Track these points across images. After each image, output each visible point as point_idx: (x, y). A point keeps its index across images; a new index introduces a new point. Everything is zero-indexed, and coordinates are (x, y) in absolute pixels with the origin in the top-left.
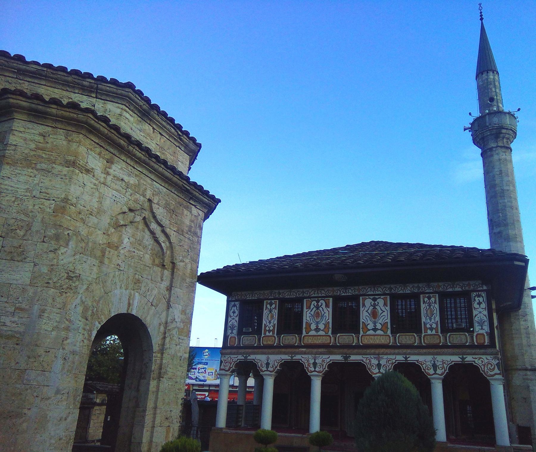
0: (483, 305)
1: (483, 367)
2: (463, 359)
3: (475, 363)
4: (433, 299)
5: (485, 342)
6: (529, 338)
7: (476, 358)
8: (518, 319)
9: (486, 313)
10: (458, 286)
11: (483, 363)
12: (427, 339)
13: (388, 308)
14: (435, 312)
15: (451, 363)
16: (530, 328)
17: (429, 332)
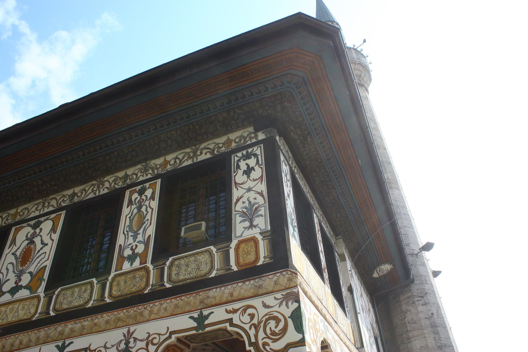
0: (257, 173)
1: (252, 332)
2: (201, 320)
3: (232, 325)
4: (149, 193)
5: (257, 258)
6: (436, 333)
7: (235, 311)
8: (413, 303)
9: (263, 187)
10: (204, 151)
11: (255, 321)
12: (118, 284)
13: (56, 237)
14: (148, 217)
15: (170, 337)
16: (435, 316)
17: (126, 266)
